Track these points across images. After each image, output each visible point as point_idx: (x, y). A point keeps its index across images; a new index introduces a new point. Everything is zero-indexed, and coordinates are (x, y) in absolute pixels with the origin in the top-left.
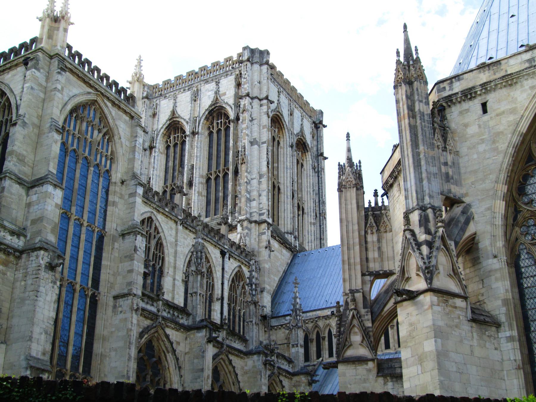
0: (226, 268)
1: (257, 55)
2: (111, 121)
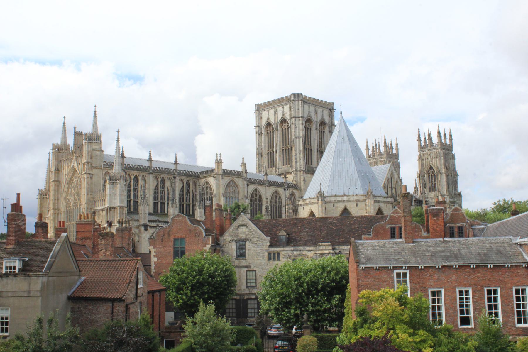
0: (286, 194)
1: (297, 97)
2: (237, 183)
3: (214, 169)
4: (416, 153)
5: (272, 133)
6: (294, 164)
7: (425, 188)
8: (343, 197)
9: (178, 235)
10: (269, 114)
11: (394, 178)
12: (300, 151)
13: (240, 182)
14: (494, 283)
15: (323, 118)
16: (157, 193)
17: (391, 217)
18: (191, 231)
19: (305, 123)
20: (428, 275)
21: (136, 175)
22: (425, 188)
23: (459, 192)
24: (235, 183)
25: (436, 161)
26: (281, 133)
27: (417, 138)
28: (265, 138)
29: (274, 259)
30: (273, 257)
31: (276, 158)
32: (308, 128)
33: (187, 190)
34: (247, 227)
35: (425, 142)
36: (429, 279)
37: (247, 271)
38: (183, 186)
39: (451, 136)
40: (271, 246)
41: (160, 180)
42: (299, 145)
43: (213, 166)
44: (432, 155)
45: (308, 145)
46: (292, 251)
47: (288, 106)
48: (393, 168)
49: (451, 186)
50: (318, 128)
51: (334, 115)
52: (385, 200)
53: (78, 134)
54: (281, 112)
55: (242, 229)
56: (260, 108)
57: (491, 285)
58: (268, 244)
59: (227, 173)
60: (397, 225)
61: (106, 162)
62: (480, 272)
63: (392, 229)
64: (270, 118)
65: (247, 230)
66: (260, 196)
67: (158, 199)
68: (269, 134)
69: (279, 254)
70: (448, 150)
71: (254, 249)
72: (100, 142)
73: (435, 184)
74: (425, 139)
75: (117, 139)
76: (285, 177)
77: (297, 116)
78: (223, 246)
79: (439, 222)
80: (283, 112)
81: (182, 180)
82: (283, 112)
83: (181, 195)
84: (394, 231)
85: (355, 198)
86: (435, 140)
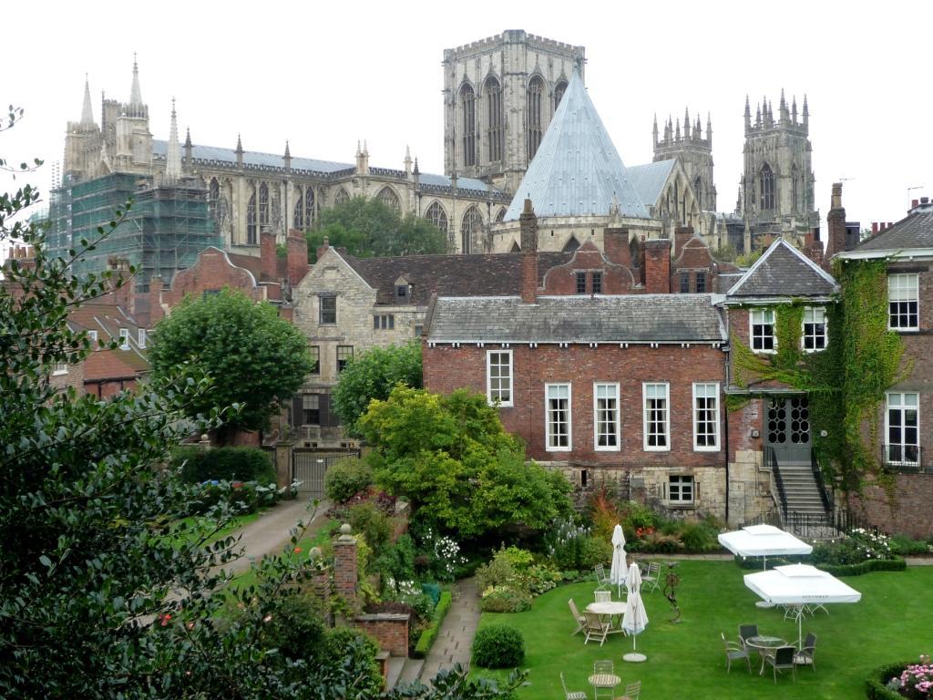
0: (492, 212)
1: (514, 36)
3: (354, 169)
4: (741, 140)
5: (471, 103)
6: (506, 159)
7: (753, 202)
8: (567, 219)
9: (210, 285)
10: (466, 68)
11: (681, 184)
12: (519, 136)
13: (401, 191)
14: (659, 375)
15: (563, 74)
16: (255, 209)
17: (599, 254)
18: (231, 278)
19: (530, 84)
20: (545, 360)
21: (214, 178)
22: (753, 202)
23: (816, 210)
24: (392, 192)
25: (776, 155)
26: (488, 101)
27: (743, 112)
28: (459, 112)
29: (384, 326)
30: (384, 322)
31: (478, 148)
32: (535, 94)
33: (308, 204)
34: (338, 271)
35: (758, 120)
36: (547, 367)
37: (338, 346)
38: (302, 197)
39: (805, 108)
40: (380, 304)
41: (258, 186)
42: (516, 125)
43: (352, 161)
44: (769, 143)
45: (535, 124)
46: (415, 312)
47: (500, 53)
48: (679, 166)
49: (800, 200)
50: (554, 93)
51: (584, 70)
52: (645, 224)
53: (108, 105)
54: (488, 64)
55: (331, 275)
56: (452, 58)
57: (654, 377)
58: (374, 301)
59: (379, 174)
60: (590, 270)
61: (157, 154)
62: (634, 356)
63: (581, 277)
64: (469, 74)
65: (339, 277)
66: (444, 216)
67: (255, 220)
68: (467, 105)
69: (392, 318)
70: (799, 134)
71: (351, 308)
72: (145, 119)
73: (772, 196)
74: (759, 113)
75: (171, 114)
76: (490, 183)
77: (515, 71)
78: (298, 303)
79: (660, 265)
80: (491, 64)
81: (298, 188)
82: (491, 64)
83: (298, 213)
84: (584, 281)
85: (591, 220)
86: (777, 116)
